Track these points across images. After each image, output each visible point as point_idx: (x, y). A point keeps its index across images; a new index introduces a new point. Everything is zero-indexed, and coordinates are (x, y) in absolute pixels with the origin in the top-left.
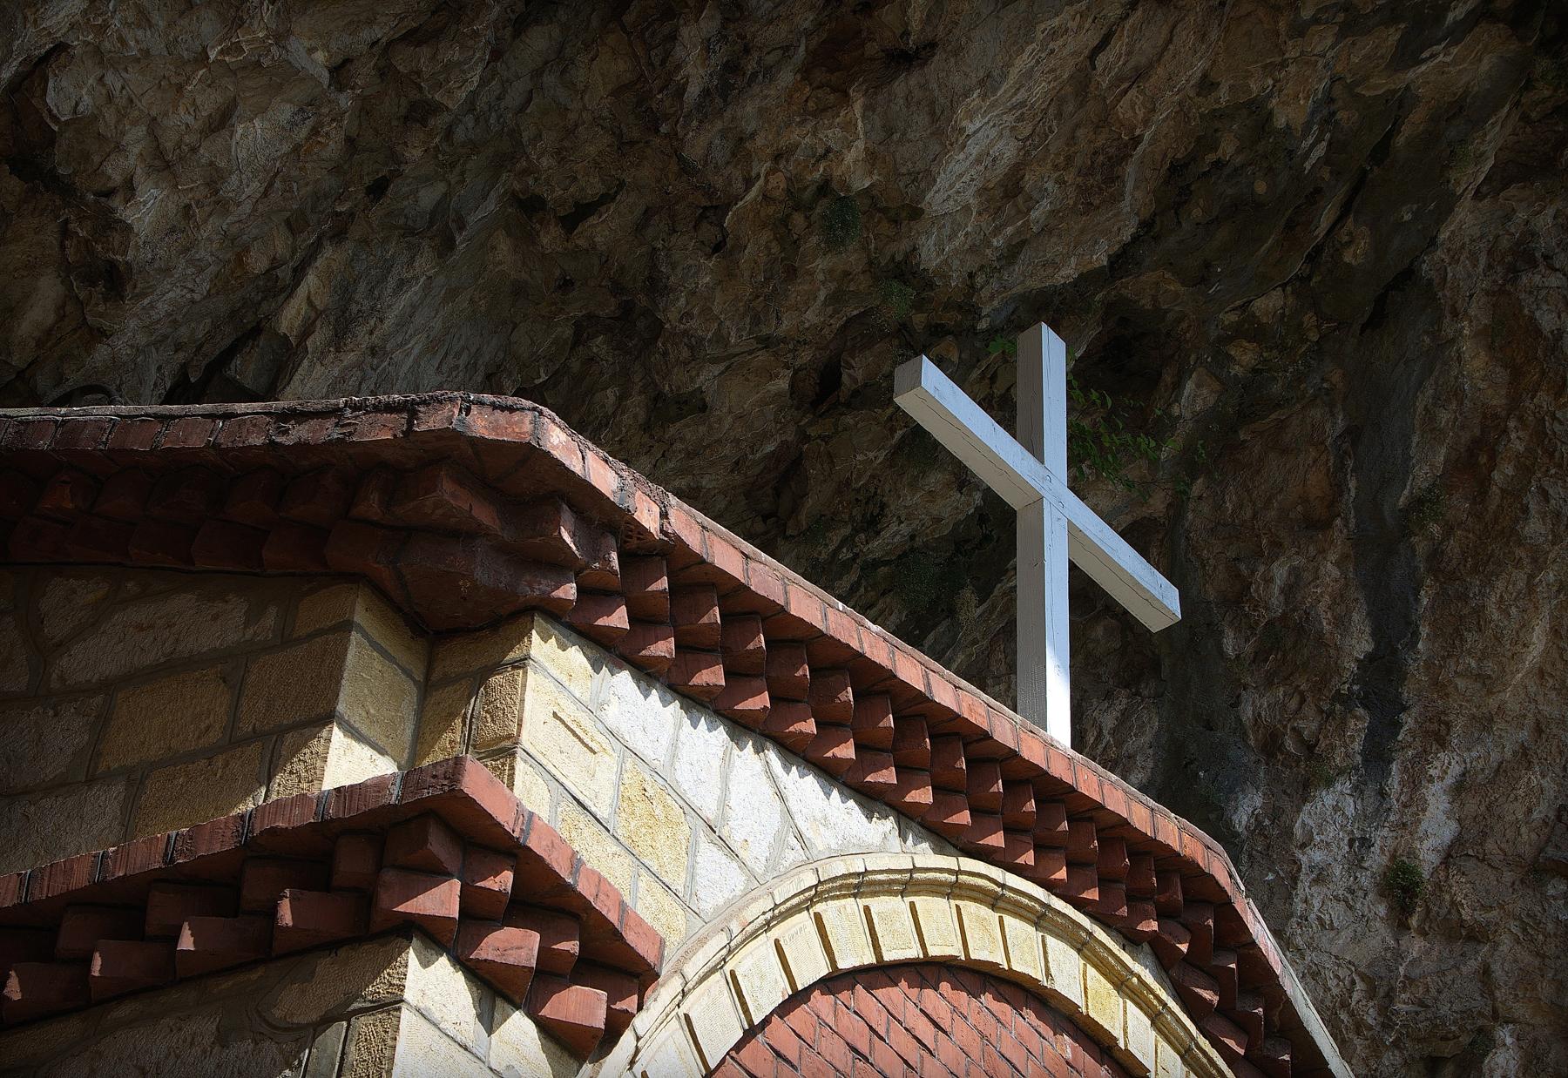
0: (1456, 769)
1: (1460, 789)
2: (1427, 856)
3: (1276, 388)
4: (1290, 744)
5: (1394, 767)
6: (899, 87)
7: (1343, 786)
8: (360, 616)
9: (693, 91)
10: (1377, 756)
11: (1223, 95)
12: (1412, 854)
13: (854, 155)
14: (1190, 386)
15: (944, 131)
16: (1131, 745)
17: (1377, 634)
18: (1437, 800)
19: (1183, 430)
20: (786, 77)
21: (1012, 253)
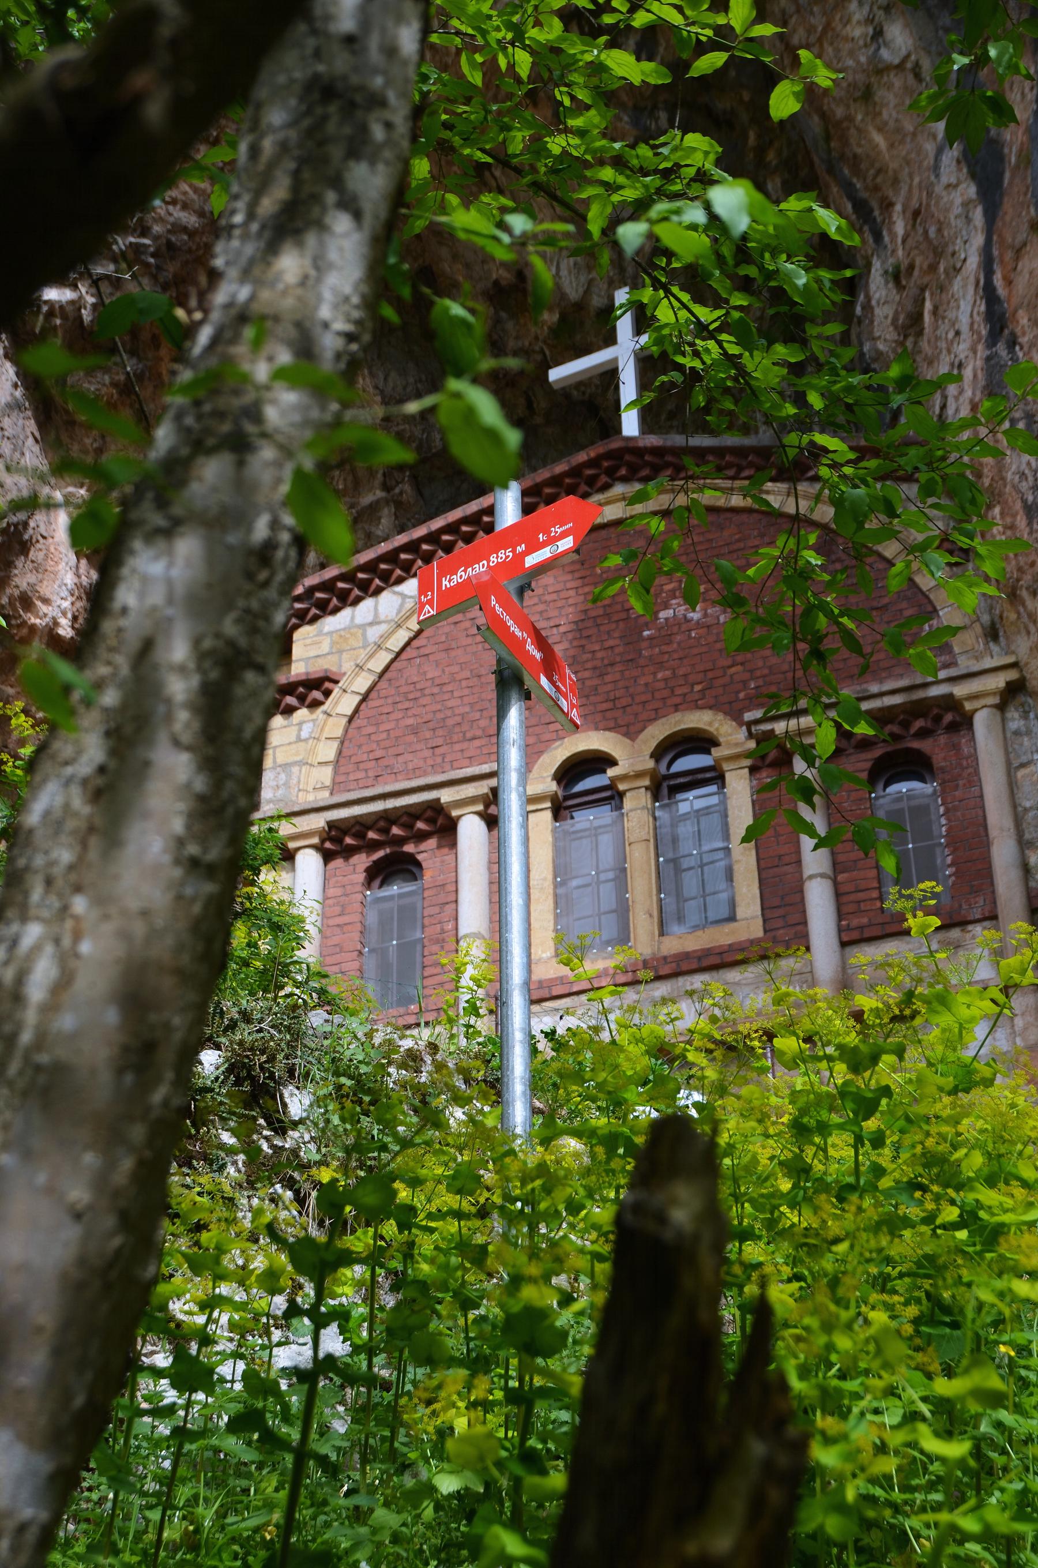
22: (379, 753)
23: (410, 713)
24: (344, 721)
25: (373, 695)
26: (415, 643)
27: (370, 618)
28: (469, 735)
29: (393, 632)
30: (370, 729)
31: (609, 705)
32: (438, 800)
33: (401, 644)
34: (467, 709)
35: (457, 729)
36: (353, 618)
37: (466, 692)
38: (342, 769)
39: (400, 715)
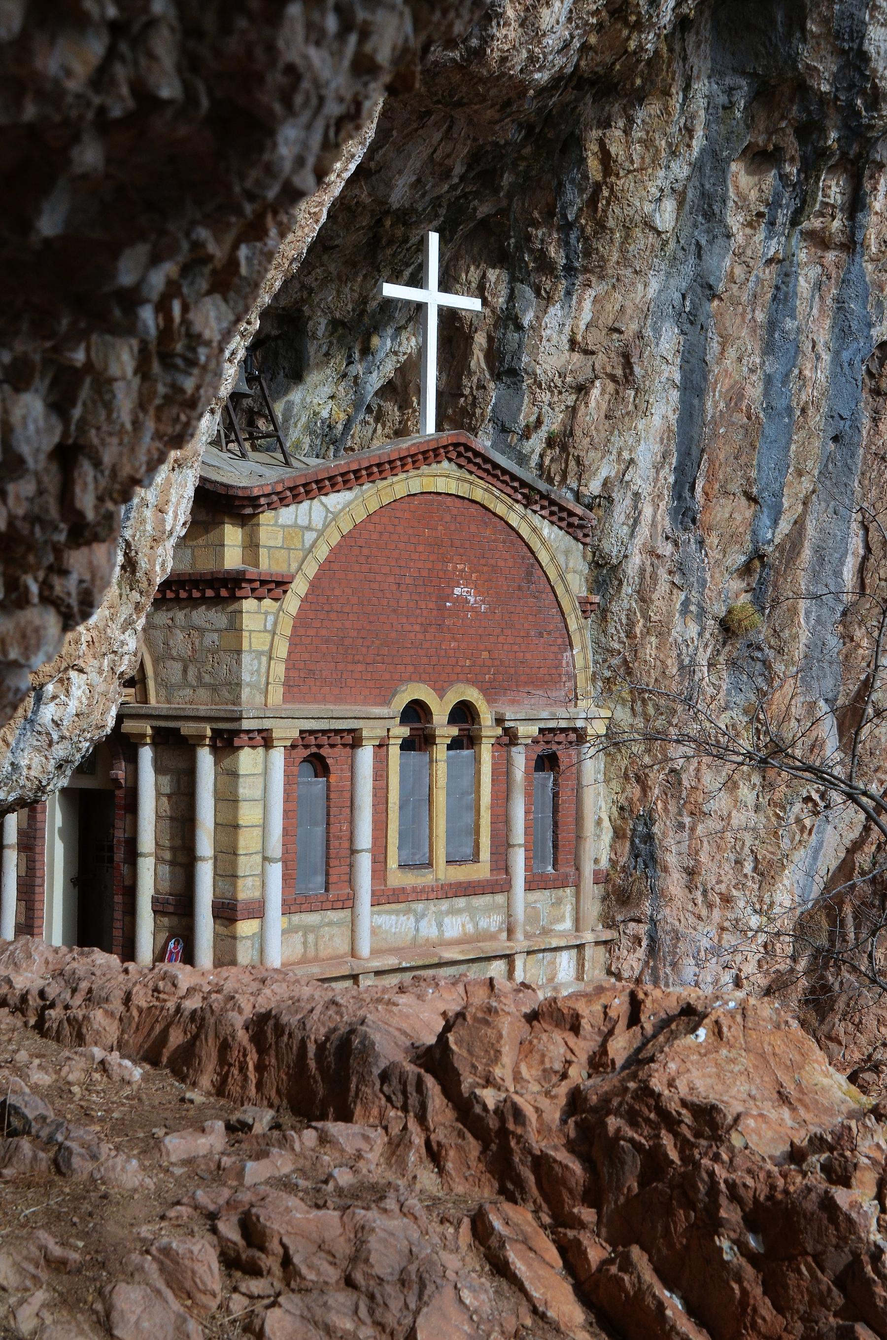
0: (594, 294)
1: (595, 301)
2: (582, 327)
3: (534, 173)
4: (543, 292)
5: (574, 297)
6: (373, 178)
7: (558, 306)
8: (226, 520)
10: (569, 293)
11: (481, 142)
12: (577, 327)
14: (506, 175)
15: (389, 186)
16: (499, 288)
17: (567, 257)
18: (587, 305)
19: (506, 188)
21: (423, 195)
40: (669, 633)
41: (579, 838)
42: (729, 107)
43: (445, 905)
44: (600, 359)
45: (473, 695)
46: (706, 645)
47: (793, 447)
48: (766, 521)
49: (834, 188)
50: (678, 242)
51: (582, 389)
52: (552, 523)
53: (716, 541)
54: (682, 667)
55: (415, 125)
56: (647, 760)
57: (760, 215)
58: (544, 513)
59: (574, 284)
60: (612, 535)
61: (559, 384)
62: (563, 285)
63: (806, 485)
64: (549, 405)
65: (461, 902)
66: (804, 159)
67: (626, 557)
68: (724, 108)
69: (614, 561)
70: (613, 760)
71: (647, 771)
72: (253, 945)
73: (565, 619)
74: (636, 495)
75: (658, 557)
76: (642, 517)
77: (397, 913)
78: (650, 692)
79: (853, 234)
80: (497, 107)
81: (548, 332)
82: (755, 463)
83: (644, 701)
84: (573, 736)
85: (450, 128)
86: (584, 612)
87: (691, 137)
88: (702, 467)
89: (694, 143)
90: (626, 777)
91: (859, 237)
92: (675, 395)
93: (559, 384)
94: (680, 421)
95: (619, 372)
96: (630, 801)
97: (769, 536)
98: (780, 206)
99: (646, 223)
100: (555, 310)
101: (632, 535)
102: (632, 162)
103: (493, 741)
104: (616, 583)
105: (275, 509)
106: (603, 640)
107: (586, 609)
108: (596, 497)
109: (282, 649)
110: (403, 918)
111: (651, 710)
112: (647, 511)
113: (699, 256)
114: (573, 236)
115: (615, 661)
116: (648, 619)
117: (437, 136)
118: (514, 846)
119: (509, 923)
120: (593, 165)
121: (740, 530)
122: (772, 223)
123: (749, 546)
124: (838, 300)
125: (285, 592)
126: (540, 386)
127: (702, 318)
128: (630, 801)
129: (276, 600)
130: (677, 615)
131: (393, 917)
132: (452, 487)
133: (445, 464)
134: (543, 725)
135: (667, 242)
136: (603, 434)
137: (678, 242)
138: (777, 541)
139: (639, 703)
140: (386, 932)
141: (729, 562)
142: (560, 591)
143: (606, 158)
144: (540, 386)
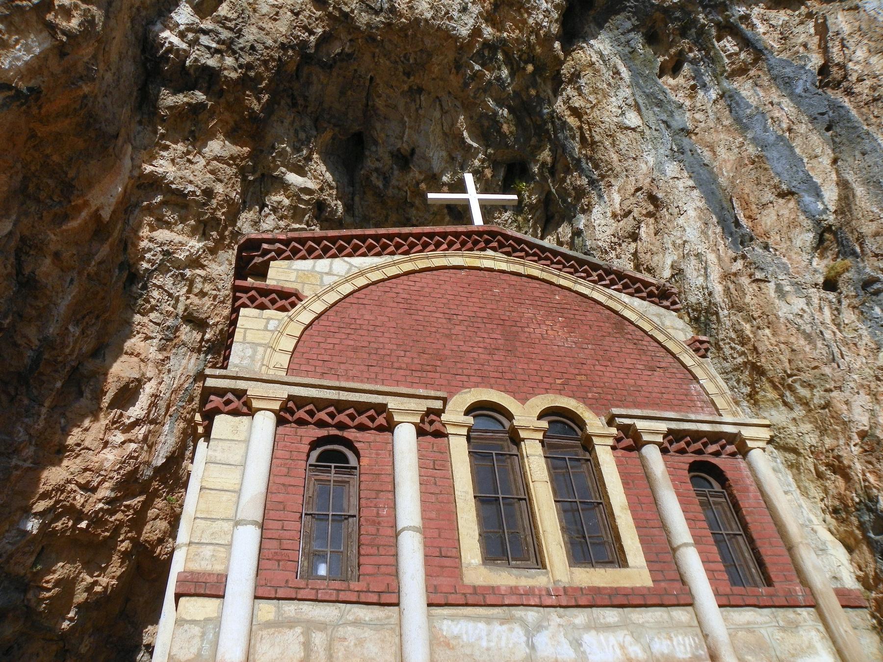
6: (415, 159)
7: (597, 206)
9: (381, 186)
10: (600, 197)
11: (475, 118)
13: (417, 175)
15: (427, 160)
20: (396, 172)
22: (326, 358)
23: (351, 337)
24: (302, 327)
25: (323, 317)
26: (356, 294)
27: (327, 270)
28: (396, 365)
29: (343, 283)
30: (320, 339)
31: (500, 375)
32: (386, 405)
33: (348, 292)
34: (395, 347)
35: (387, 358)
36: (314, 266)
37: (394, 336)
38: (296, 360)
39: (344, 336)
40: (778, 317)
41: (790, 548)
42: (633, 51)
43: (580, 617)
44: (636, 213)
45: (570, 404)
46: (821, 309)
47: (797, 150)
48: (807, 199)
49: (728, 45)
50: (650, 128)
51: (634, 237)
52: (631, 295)
53: (778, 238)
54: (808, 337)
55: (413, 107)
56: (829, 442)
57: (693, 88)
58: (619, 286)
59: (600, 189)
60: (693, 288)
61: (616, 240)
62: (594, 195)
63: (826, 161)
64: (617, 257)
65: (611, 615)
66: (696, 43)
67: (710, 294)
68: (631, 53)
69: (705, 304)
70: (798, 469)
71: (836, 452)
72: (203, 634)
73: (678, 359)
74: (698, 256)
75: (735, 274)
76: (709, 262)
77: (488, 620)
78: (789, 376)
79: (755, 48)
80: (454, 70)
81: (598, 222)
82: (773, 175)
83: (790, 388)
84: (731, 448)
85: (441, 105)
86: (697, 350)
87: (619, 74)
88: (735, 205)
89: (623, 75)
90: (820, 476)
91: (759, 46)
92: (696, 193)
93: (616, 240)
94: (708, 201)
95: (651, 208)
96: (841, 498)
97: (821, 207)
98: (703, 74)
99: (620, 127)
100: (597, 211)
101: (706, 276)
102: (591, 102)
103: (611, 442)
104: (714, 317)
105: (288, 258)
106: (727, 365)
107: (698, 348)
108: (671, 279)
109: (289, 344)
110: (497, 628)
111: (803, 392)
112: (711, 257)
113: (668, 126)
114: (584, 165)
115: (745, 376)
116: (750, 319)
117: (437, 114)
118: (679, 547)
119: (709, 648)
120: (572, 121)
121: (792, 217)
122: (704, 86)
123: (808, 223)
124: (774, 79)
125: (293, 305)
126: (606, 252)
127: (687, 148)
128: (841, 498)
129: (283, 309)
130: (777, 301)
131: (482, 626)
132: (503, 266)
133: (490, 252)
134: (674, 426)
135: (643, 131)
136: (658, 243)
137: (650, 128)
138: (832, 208)
139: (788, 393)
140: (472, 645)
141: (799, 243)
142: (661, 338)
143: (576, 112)
144: (606, 252)
